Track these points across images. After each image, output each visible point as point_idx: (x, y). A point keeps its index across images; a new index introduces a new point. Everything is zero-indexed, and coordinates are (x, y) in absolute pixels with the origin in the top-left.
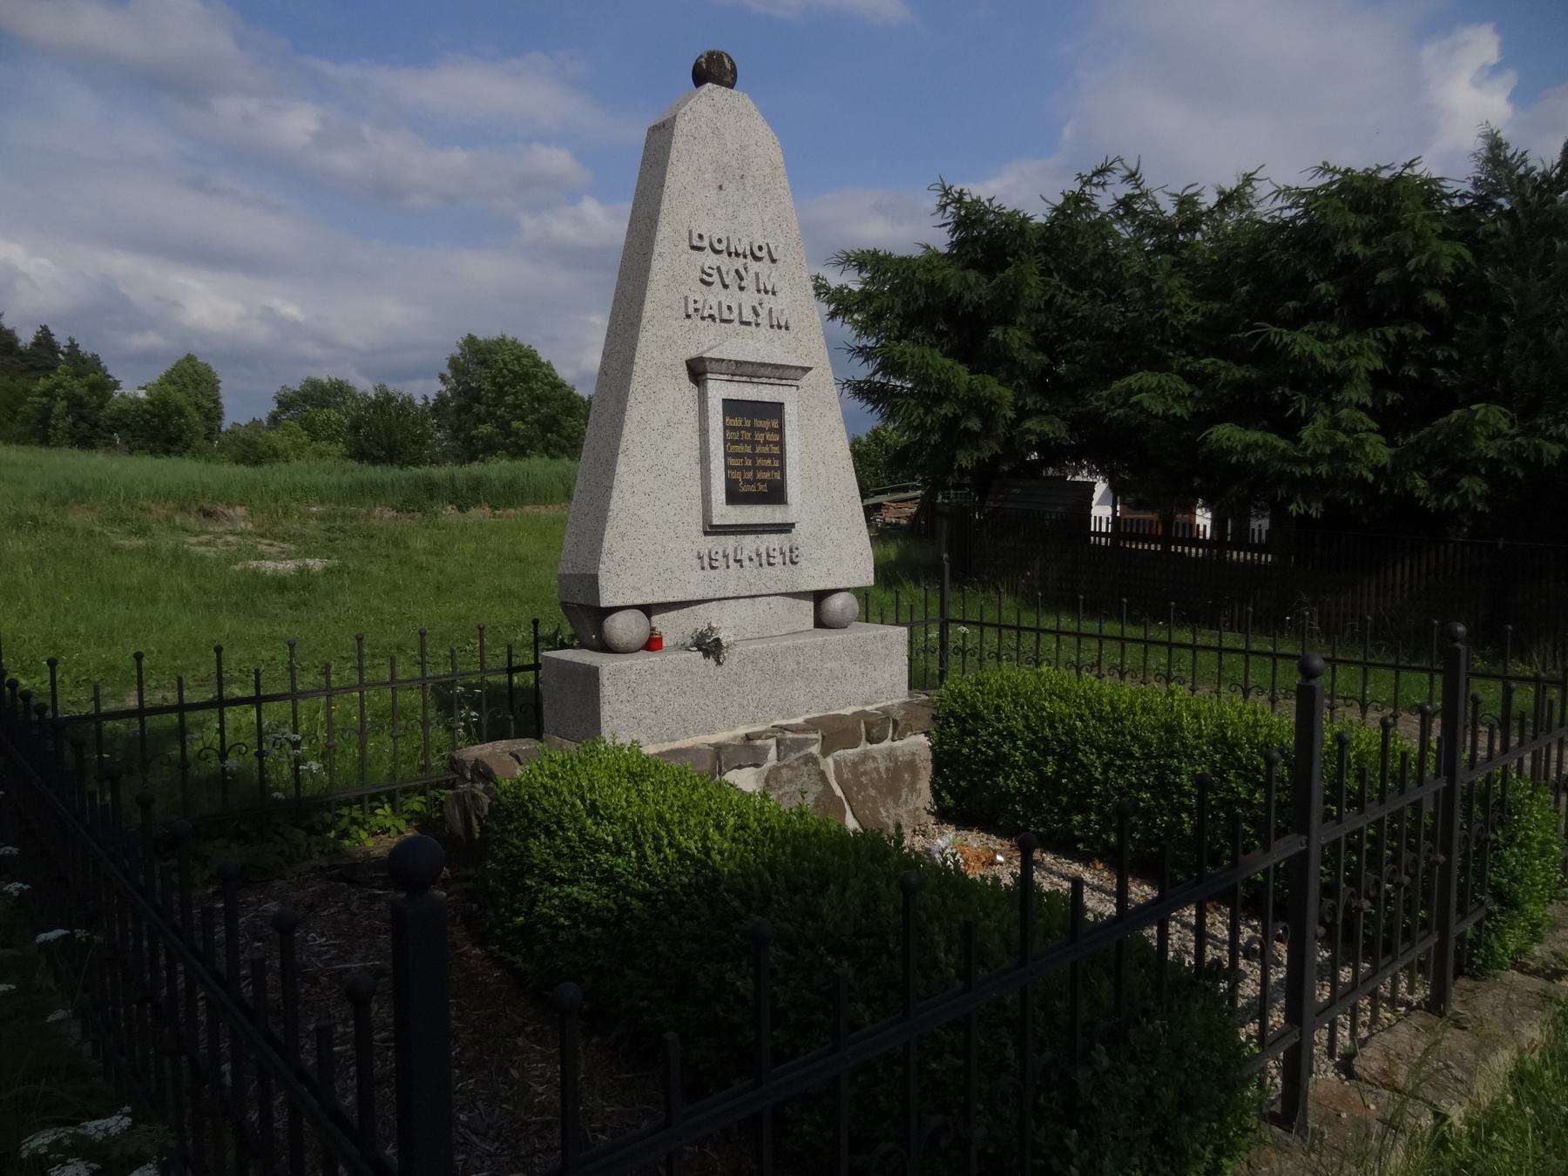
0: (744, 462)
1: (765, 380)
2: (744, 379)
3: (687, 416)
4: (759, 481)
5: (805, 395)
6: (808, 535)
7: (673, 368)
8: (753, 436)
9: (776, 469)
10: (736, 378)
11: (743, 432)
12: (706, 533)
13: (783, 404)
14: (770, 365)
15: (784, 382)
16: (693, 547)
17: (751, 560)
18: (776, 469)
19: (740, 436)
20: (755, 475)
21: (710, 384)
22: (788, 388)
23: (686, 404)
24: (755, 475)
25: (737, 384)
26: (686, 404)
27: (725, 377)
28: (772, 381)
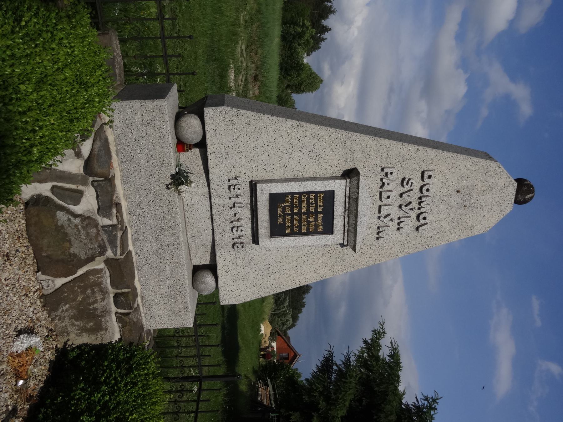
0: (296, 207)
1: (347, 220)
2: (347, 205)
3: (323, 169)
4: (285, 217)
5: (338, 252)
6: (252, 255)
7: (351, 159)
8: (312, 213)
9: (292, 230)
10: (347, 200)
11: (314, 205)
12: (251, 182)
13: (332, 234)
14: (356, 222)
15: (346, 234)
16: (242, 173)
17: (235, 215)
18: (292, 230)
19: (312, 204)
20: (288, 215)
21: (343, 182)
22: (342, 237)
23: (330, 167)
24: (288, 215)
25: (343, 201)
26: (330, 167)
27: (348, 192)
28: (347, 225)
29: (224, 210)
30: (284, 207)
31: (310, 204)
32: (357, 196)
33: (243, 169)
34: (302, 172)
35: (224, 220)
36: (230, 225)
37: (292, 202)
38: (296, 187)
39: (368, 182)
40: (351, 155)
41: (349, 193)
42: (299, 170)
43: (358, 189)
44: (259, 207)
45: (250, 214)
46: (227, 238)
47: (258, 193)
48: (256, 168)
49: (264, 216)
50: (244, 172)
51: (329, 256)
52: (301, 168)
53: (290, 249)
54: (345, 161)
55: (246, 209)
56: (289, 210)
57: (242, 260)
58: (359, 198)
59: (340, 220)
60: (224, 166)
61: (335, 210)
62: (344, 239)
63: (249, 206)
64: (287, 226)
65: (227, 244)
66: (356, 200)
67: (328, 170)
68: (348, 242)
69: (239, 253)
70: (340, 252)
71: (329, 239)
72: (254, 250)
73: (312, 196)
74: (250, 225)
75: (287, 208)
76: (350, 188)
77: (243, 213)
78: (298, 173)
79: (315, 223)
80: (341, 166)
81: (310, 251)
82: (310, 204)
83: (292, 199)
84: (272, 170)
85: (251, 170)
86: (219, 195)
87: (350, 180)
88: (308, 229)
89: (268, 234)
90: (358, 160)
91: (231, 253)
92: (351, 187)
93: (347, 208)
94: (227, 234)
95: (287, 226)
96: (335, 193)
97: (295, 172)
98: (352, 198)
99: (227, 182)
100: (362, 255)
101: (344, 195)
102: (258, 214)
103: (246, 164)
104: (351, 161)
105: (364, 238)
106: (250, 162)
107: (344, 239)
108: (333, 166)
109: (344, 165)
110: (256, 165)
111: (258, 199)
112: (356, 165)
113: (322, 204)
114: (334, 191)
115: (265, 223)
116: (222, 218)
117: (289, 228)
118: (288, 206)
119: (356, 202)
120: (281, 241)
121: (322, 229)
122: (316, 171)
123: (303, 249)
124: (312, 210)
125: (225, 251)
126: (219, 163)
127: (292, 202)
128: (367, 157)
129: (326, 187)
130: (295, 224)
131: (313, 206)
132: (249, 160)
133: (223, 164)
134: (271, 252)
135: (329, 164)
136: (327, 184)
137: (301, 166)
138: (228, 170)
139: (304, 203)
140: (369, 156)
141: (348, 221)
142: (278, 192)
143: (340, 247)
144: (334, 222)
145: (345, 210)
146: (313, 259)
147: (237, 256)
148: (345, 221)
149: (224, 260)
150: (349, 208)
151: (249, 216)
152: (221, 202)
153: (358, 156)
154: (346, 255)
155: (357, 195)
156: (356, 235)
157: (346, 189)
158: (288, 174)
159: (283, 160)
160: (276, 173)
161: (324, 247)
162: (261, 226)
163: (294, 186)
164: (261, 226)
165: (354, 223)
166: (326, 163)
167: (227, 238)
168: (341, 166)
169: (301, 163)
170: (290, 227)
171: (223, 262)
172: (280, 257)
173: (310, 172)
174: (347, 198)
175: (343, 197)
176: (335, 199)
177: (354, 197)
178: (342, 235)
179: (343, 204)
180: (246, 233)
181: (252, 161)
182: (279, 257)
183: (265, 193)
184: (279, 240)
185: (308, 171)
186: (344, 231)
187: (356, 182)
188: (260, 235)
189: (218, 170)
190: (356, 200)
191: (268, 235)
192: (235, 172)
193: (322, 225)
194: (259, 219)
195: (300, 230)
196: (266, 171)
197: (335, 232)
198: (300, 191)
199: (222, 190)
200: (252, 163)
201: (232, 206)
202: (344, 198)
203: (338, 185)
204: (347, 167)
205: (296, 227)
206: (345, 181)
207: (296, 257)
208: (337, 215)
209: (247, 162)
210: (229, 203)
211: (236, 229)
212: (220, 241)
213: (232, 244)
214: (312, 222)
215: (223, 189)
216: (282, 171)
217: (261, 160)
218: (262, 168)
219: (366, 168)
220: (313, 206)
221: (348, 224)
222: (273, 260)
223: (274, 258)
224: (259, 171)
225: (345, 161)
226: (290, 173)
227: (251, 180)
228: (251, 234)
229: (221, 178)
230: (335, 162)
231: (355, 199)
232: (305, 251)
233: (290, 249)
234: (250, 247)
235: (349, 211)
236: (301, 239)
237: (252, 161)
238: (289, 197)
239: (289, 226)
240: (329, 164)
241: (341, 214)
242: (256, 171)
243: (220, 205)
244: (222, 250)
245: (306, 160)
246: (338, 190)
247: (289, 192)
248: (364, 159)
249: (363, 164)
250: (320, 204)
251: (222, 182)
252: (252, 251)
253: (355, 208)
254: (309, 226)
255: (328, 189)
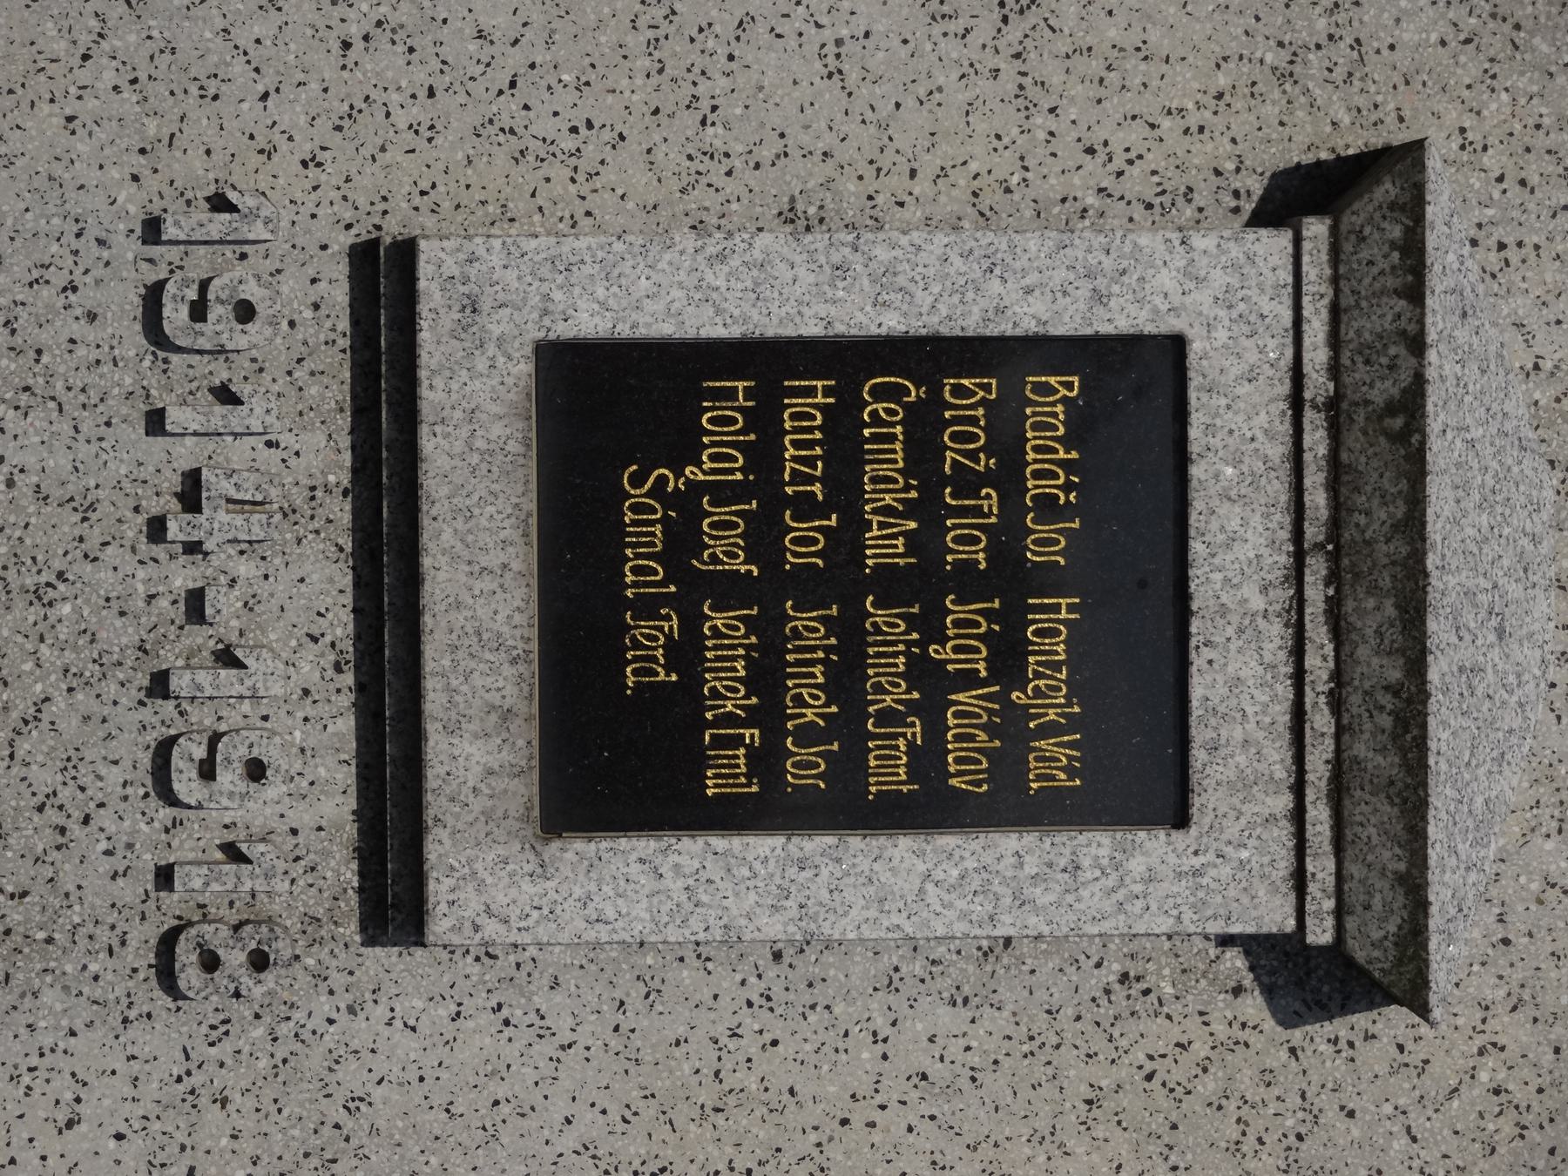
0: (806, 507)
1: (1319, 664)
2: (1317, 499)
3: (1070, 153)
4: (693, 622)
5: (1246, 1082)
6: (352, 1077)
7: (1342, 53)
8: (968, 582)
9: (766, 761)
10: (1316, 440)
11: (990, 499)
12: (364, 256)
13: (1181, 820)
14: (1416, 661)
15: (1319, 815)
16: (287, 161)
18: (766, 761)
19: (967, 483)
20: (728, 590)
21: (1273, 244)
22: (1285, 864)
23: (1135, 135)
24: (728, 590)
25: (1278, 450)
26: (1135, 135)
27: (1317, 355)
28: (1321, 720)
29: (92, 545)
30: (686, 506)
31: (944, 481)
32: (1405, 378)
33: (290, 112)
34: (869, 172)
35: (80, 659)
36: (145, 714)
37: (764, 456)
38: (808, 278)
39: (1521, 306)
40: (1341, 17)
41: (1335, 370)
42: (843, 153)
43: (1415, 293)
44: (433, 484)
45: (348, 599)
46: (106, 865)
47: (425, 336)
48: (416, 113)
49: (487, 584)
50: (305, 150)
51: (1158, 1124)
52: (851, 127)
53: (750, 1024)
54: (1284, 76)
55: (313, 545)
56: (735, 536)
57: (247, 1124)
58: (1437, 417)
59: (1250, 669)
60: (109, 77)
61: (1197, 547)
62: (1300, 880)
63: (342, 512)
64: (719, 721)
65: (104, 936)
66: (1398, 423)
67: (1119, 162)
68: (1340, 913)
69: (227, 1046)
70: (1267, 1077)
71: (1150, 878)
72: (381, 1012)
73: (959, 391)
74: (346, 725)
75: (723, 512)
76: (1335, 311)
77: (281, 586)
78: (827, 184)
79: (1002, 698)
80: (1242, 124)
81: (955, 1049)
82: (944, 481)
83: (765, 419)
84: (569, 143)
85: (369, 127)
86: (50, 376)
87: (1334, 231)
88: (927, 759)
89: (523, 792)
90: (1405, 64)
91: (143, 1038)
92: (1347, 300)
93: (1314, 532)
94: (104, 818)
95: (719, 721)
96: (1192, 359)
97: (796, 164)
98: (1360, 417)
99: (129, 248)
100: (1507, 1127)
101: (1285, 388)
102: (426, 562)
103: (327, 65)
104: (1339, 74)
105: (1517, 926)
106: (358, 44)
107: (1300, 880)
108: (1166, 123)
109: (1271, 111)
110: (421, 76)
111: (430, 397)
112: (1391, 119)
113: (1068, 487)
114: (1178, 343)
115: (494, 670)
116: (63, 632)
117: (737, 741)
118: (723, 493)
119: (1401, 437)
120: (646, 882)
121: (1071, 772)
122: (1005, 164)
123: (881, 1023)
124: (963, 553)
125: (85, 1012)
126: (60, 47)
127: (764, 456)
128: (1496, 44)
129: (1099, 298)
130: (799, 701)
131: (977, 511)
132: (354, 31)
133: (100, 60)
134: (548, 1048)
135: (1131, 103)
136: (1108, 263)
137: (859, 106)
138: (152, 127)
139: (884, 470)
140: (1507, 28)
141: (1337, 676)
142: (624, 331)
143: (1269, 1024)
144: (1197, 692)
145: (1299, 557)
146: (986, 1151)
147: (197, 1079)
148: (1299, 677)
149: (62, 1117)
150: (1335, 524)
151: (341, 625)
152: (60, 462)
153: (1408, 34)
154: (1331, 1115)
155: (1408, 363)
156: (1423, 804)
157: (1298, 321)
158: (731, 187)
159: (677, 45)
160: (608, 176)
161: (1105, 1012)
162: (451, 691)
163: (781, 269)
164: (451, 691)
165: (1395, 675)
166: (1095, 91)
167: (106, 865)
168: (1242, 124)
169: (853, 77)
170: (751, 734)
171: (49, 1142)
172: (649, 1110)
173: (943, 173)
174: (1309, 415)
175: (1270, 415)
176: (1194, 433)
177: (1383, 391)
178: (1282, 833)
179: (1278, 489)
180: (303, 816)
181: (381, 39)
182: (638, 1105)
183: (496, 330)
184: (635, 868)
185: (929, 165)
186: (1299, 789)
187: (1396, 232)
188: (435, 804)
189: (49, 119)
190: (1398, 423)
191: (515, 807)
192: (217, 144)
193: (1073, 723)
194: (427, 620)
195: (848, 767)
196: (514, 144)
197: (1207, 800)
198: (840, 328)
199: (78, 329)
200: (385, 62)
201: (175, 505)
202: (1286, 428)
203: (1219, 279)
204: (1301, 139)
205: (807, 735)
206: (1284, 238)
207: (813, 1114)
208: (1223, 611)
209: (336, 46)
210: (147, 472)
211: (200, 752)
212: (39, 889)
213: (152, 932)
214: (968, 680)
215: (92, 317)
216: (671, 157)
217: (470, 31)
218: (473, 118)
219: (1486, 160)
220: (977, 511)
221: (1336, 704)
222: (569, 1141)
223: (588, 1125)
224: (450, 147)
225: (1284, 76)
226: (751, 177)
227: (362, 232)
228: (351, 830)
229: (79, 204)
230: (1184, 86)
231: (1391, 409)
232: (911, 1053)
233: (750, 1024)
234: (338, 980)
235: (1335, 558)
236: (864, 865)
237: (381, 39)
238: (731, 394)
239: (729, 720)
240: (1131, 103)
241: (1258, 603)
242: (421, 144)
243: (57, 493)
244: (48, 997)
245: (904, 52)
246: (1221, 335)
247: (735, 332)
248: (1470, 67)
249: (1453, 116)
250: (1048, 487)
251: (88, 246)
252: (361, 1031)
253: (1400, 510)
254: (936, 729)
255: (1121, 319)
